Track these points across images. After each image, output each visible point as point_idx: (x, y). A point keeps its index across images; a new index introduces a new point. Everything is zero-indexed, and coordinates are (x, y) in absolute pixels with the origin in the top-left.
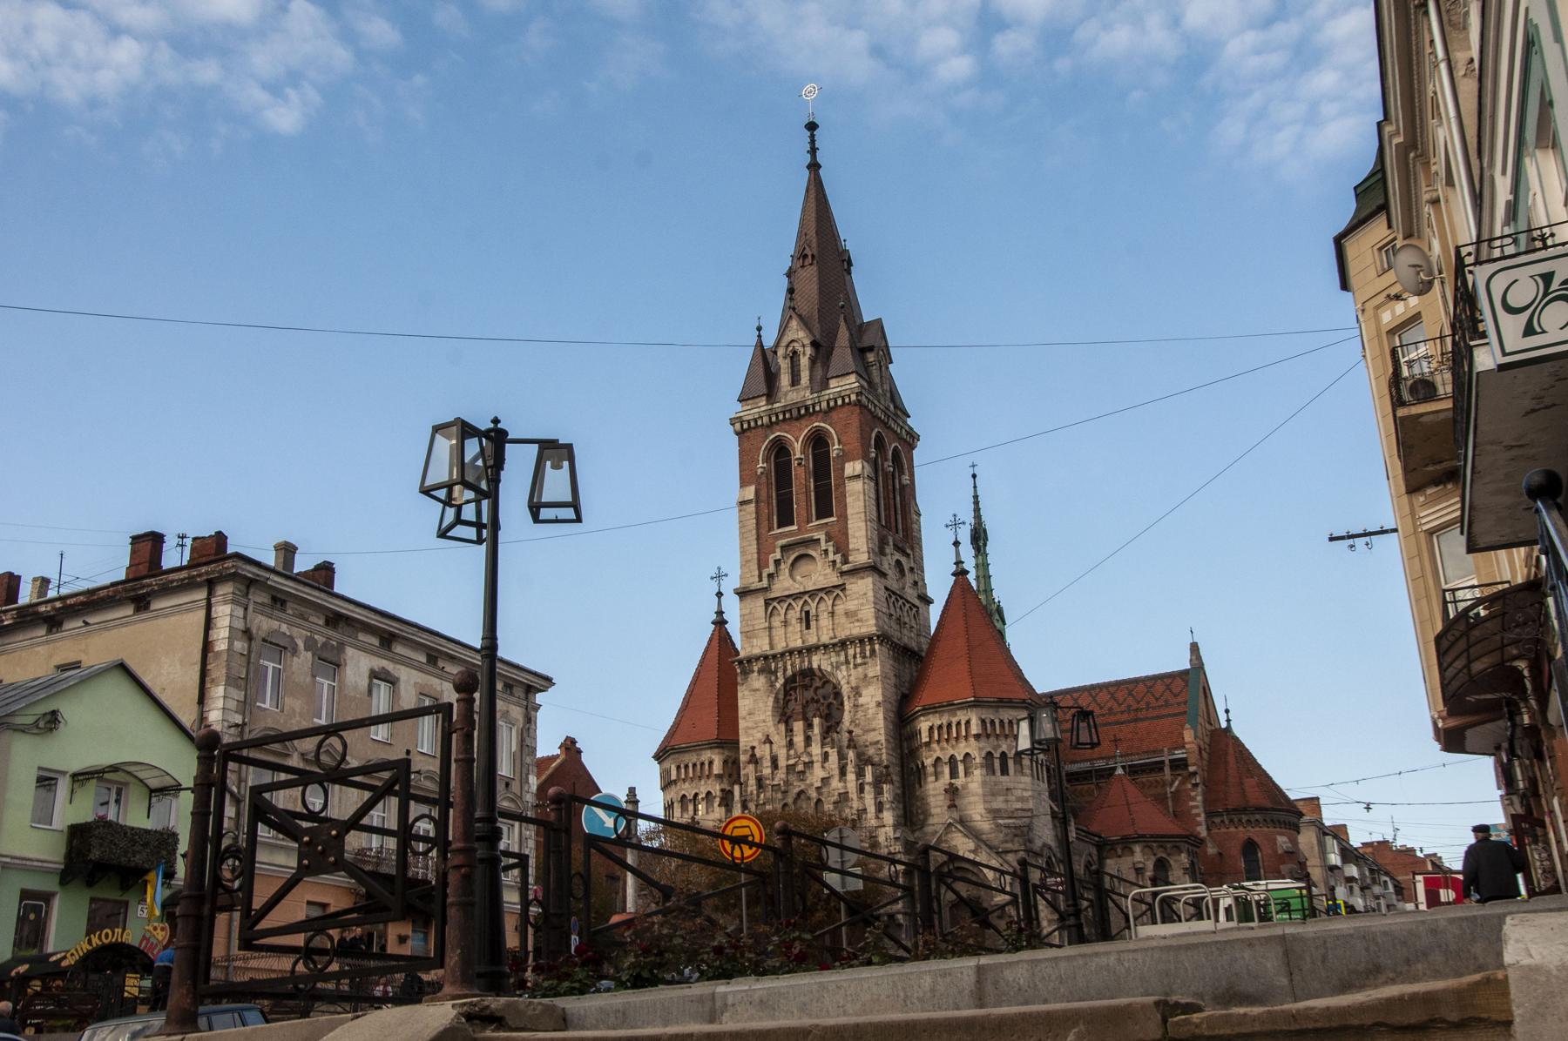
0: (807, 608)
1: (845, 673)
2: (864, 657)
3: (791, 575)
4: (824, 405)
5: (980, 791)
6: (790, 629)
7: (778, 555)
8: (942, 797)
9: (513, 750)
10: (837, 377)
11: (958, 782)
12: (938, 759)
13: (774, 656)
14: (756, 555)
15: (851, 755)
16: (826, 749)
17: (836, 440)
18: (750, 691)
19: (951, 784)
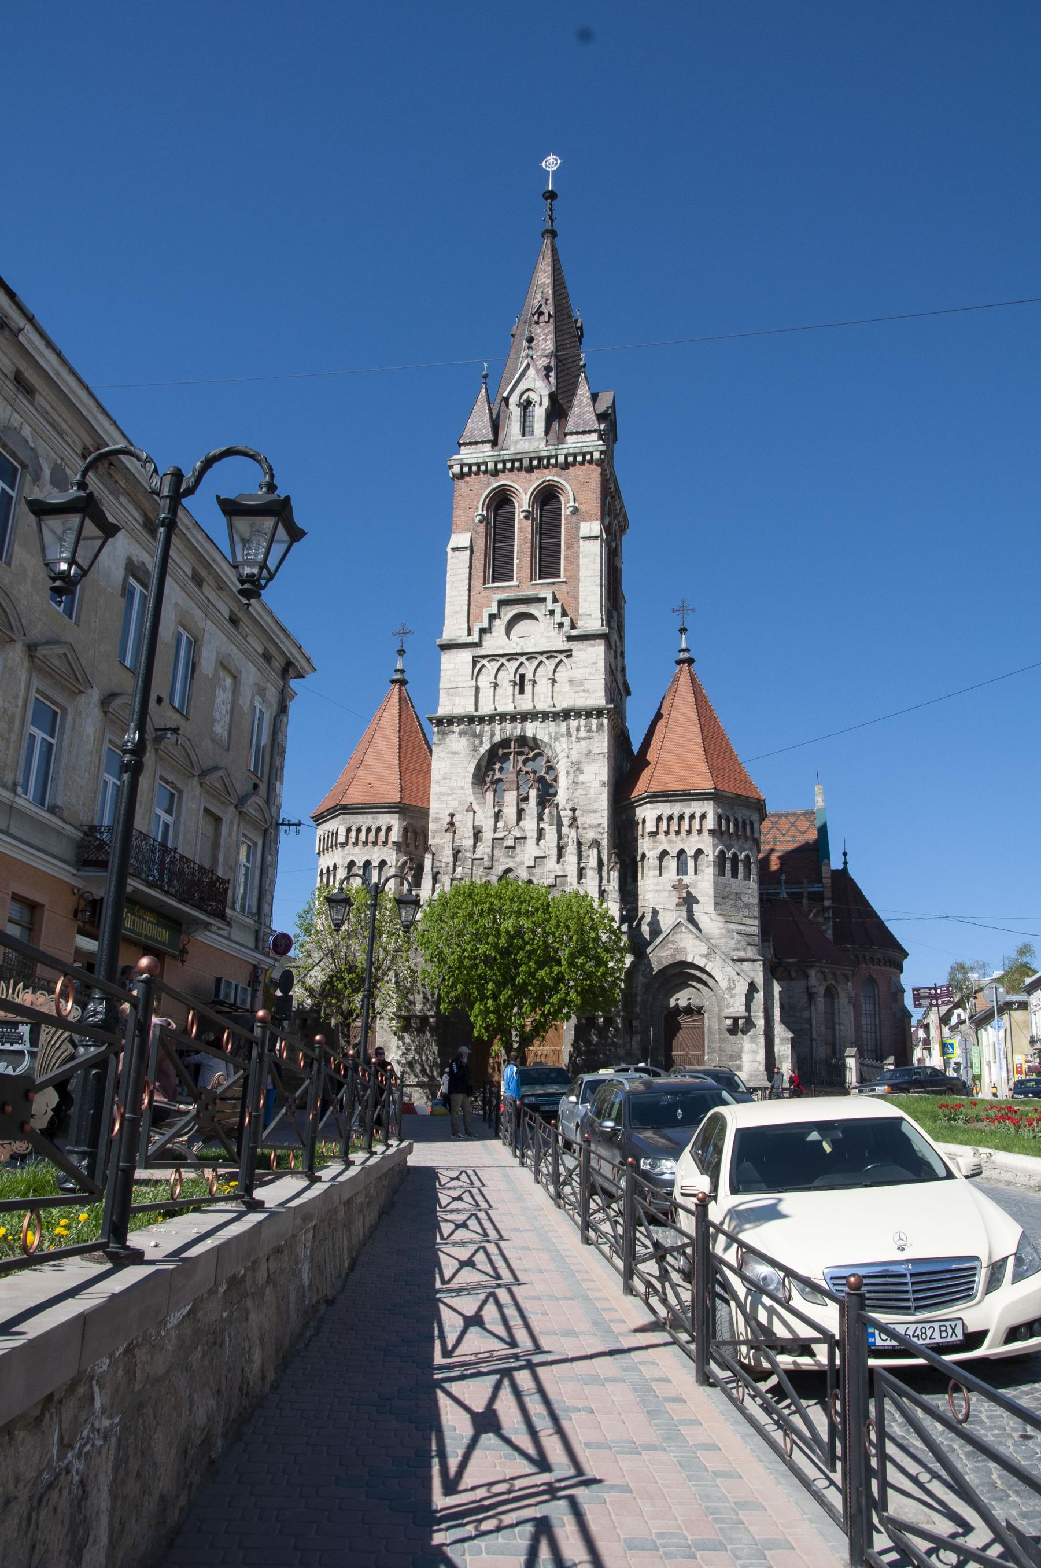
0: (521, 671)
1: (565, 746)
2: (590, 731)
3: (508, 634)
4: (561, 459)
5: (711, 892)
6: (499, 691)
7: (495, 611)
8: (666, 894)
9: (263, 743)
10: (577, 433)
11: (686, 880)
12: (664, 853)
13: (482, 720)
14: (466, 607)
15: (573, 834)
16: (541, 826)
17: (572, 498)
18: (448, 753)
19: (680, 880)
